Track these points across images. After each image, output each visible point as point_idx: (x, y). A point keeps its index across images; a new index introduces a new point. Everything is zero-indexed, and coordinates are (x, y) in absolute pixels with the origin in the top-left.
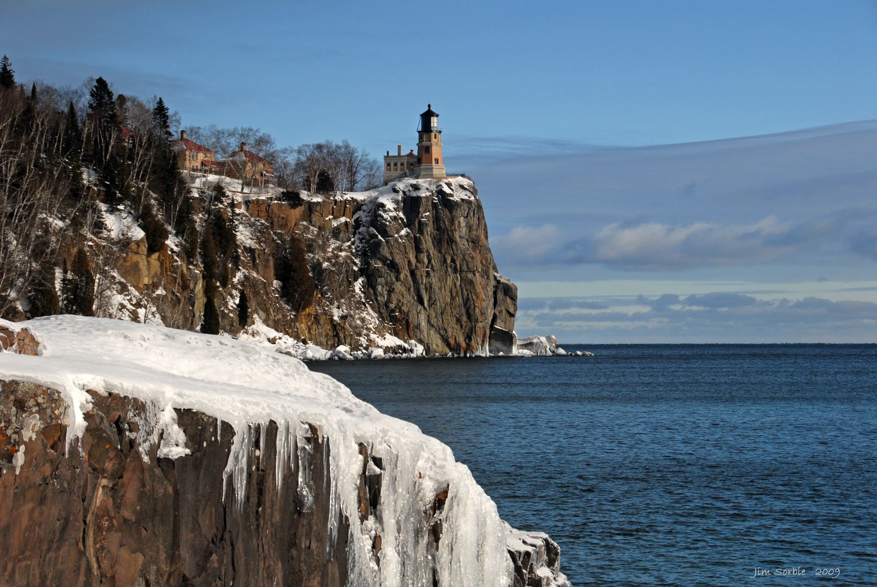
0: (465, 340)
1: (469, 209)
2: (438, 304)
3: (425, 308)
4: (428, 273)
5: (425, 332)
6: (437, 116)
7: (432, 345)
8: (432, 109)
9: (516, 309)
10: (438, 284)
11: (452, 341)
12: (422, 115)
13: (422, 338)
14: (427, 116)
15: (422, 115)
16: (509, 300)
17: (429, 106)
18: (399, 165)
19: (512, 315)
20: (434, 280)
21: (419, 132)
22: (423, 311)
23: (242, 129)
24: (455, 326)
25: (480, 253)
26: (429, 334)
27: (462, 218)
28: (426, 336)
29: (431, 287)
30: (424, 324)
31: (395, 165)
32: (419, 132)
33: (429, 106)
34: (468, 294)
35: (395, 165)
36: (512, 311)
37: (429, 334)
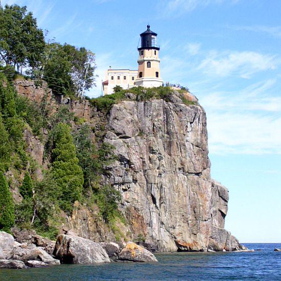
0: (190, 237)
1: (195, 115)
2: (168, 203)
3: (156, 206)
4: (160, 174)
5: (157, 228)
6: (155, 35)
7: (162, 242)
9: (227, 211)
10: (168, 185)
11: (179, 239)
13: (154, 235)
16: (222, 202)
17: (148, 27)
18: (122, 78)
19: (224, 215)
20: (165, 180)
21: (139, 49)
22: (155, 210)
23: (6, 7)
24: (182, 224)
25: (202, 157)
26: (159, 231)
27: (189, 123)
28: (157, 233)
29: (161, 187)
30: (155, 221)
31: (119, 78)
32: (139, 49)
33: (148, 27)
34: (194, 194)
35: (119, 78)
36: (223, 211)
37: (159, 231)
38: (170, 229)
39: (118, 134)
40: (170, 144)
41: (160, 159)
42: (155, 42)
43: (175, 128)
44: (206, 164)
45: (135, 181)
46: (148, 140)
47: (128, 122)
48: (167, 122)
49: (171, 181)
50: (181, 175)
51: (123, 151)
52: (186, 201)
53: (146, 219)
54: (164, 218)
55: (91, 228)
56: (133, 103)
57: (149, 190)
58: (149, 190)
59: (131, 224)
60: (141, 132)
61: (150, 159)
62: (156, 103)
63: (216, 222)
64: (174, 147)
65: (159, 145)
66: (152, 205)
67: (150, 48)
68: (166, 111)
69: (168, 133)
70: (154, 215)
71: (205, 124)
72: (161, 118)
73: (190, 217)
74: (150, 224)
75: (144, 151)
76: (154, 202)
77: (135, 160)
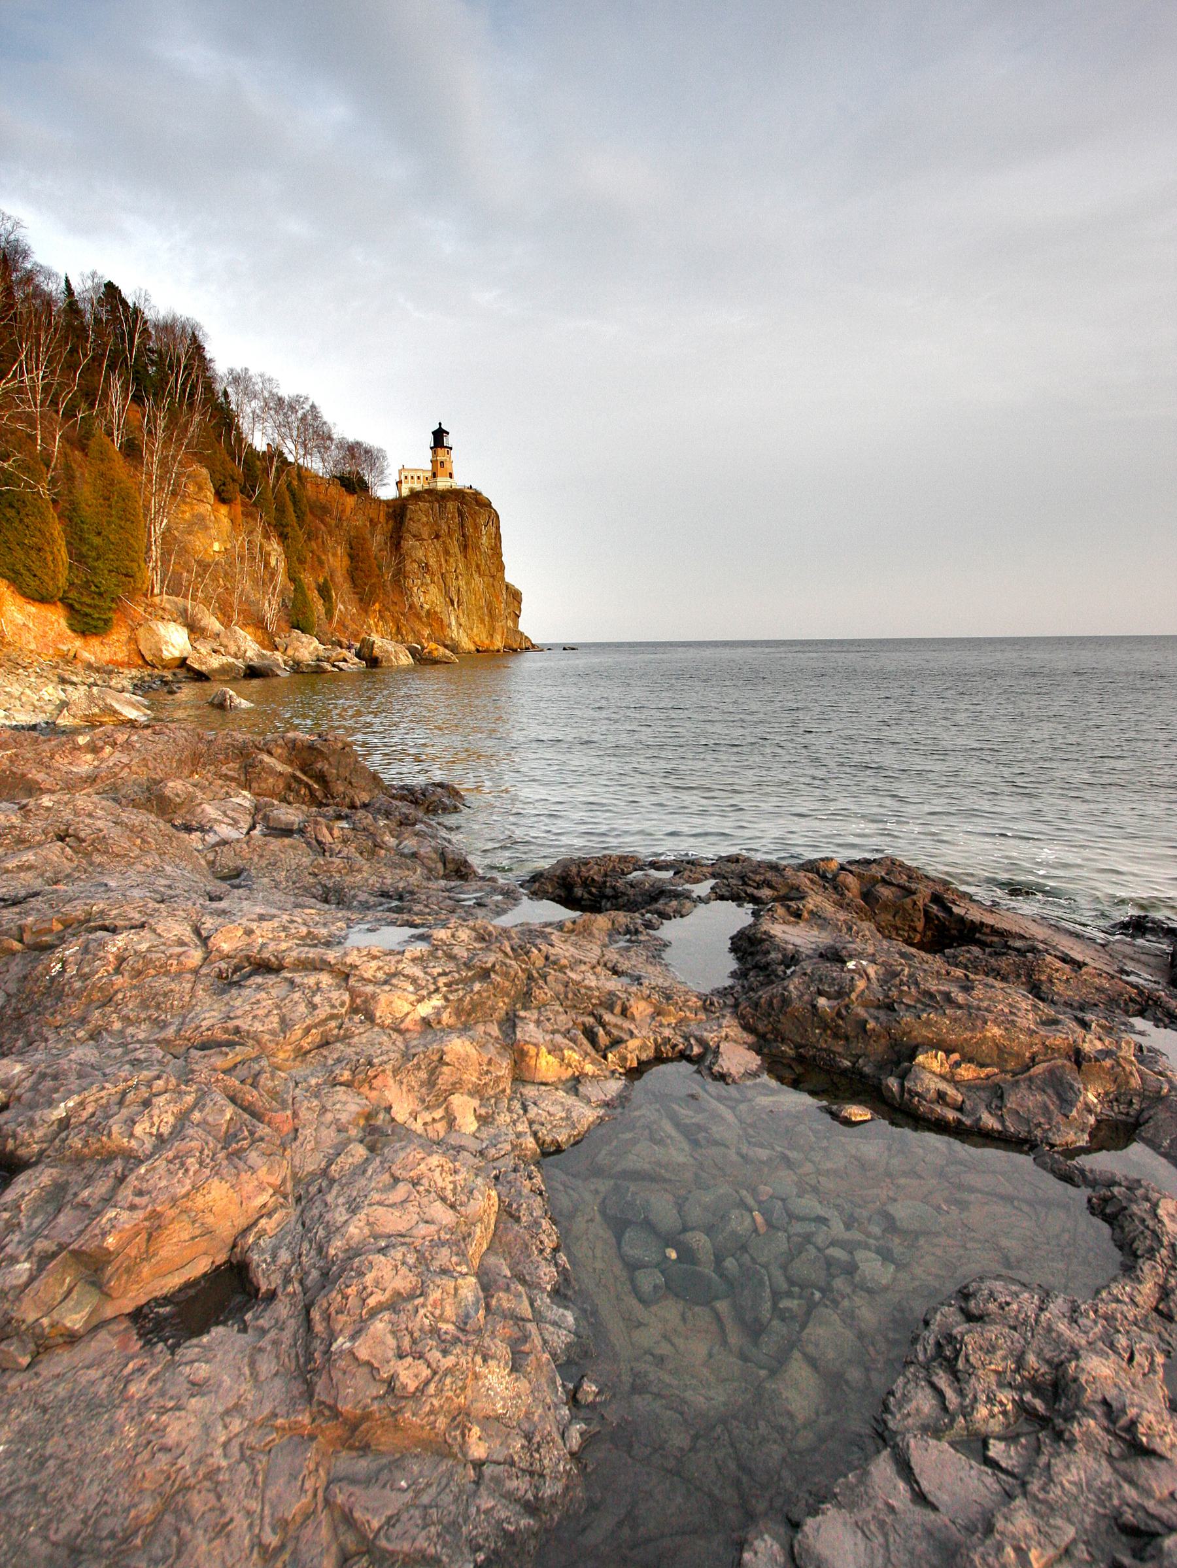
8: (443, 427)
11: (477, 639)
14: (439, 435)
16: (516, 604)
20: (462, 583)
30: (454, 623)
38: (468, 631)
39: (414, 536)
42: (448, 441)
43: (470, 531)
44: (501, 567)
47: (424, 525)
49: (468, 584)
51: (420, 554)
52: (482, 603)
53: (446, 621)
54: (463, 621)
55: (394, 631)
57: (447, 592)
58: (447, 592)
59: (431, 625)
60: (437, 537)
61: (446, 561)
62: (451, 506)
63: (510, 624)
64: (469, 550)
66: (451, 608)
67: (442, 446)
68: (461, 514)
69: (463, 536)
70: (453, 618)
71: (498, 528)
73: (487, 619)
74: (450, 625)
75: (441, 554)
76: (453, 605)
77: (432, 562)
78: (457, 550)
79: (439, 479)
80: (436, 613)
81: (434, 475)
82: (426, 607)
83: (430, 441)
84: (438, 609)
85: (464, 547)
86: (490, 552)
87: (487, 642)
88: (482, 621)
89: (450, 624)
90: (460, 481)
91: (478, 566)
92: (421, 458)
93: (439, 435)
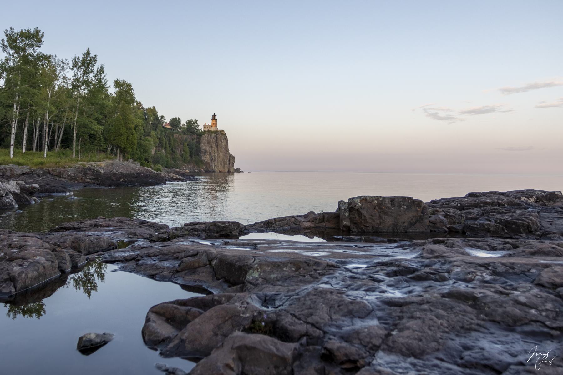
12: (213, 116)
14: (214, 116)
15: (213, 116)
40: (218, 145)
41: (214, 149)
42: (217, 118)
45: (208, 154)
46: (211, 145)
47: (206, 140)
48: (217, 140)
49: (218, 155)
50: (220, 153)
51: (204, 147)
53: (211, 164)
54: (216, 164)
56: (208, 135)
58: (211, 157)
61: (211, 149)
65: (213, 145)
68: (216, 137)
69: (217, 142)
71: (227, 140)
72: (215, 139)
73: (223, 164)
77: (208, 149)
78: (215, 146)
79: (213, 127)
80: (208, 162)
81: (212, 126)
82: (206, 161)
83: (211, 118)
84: (209, 161)
85: (217, 146)
86: (224, 147)
87: (223, 170)
88: (222, 165)
89: (212, 165)
90: (220, 128)
91: (221, 151)
92: (210, 122)
93: (214, 116)
